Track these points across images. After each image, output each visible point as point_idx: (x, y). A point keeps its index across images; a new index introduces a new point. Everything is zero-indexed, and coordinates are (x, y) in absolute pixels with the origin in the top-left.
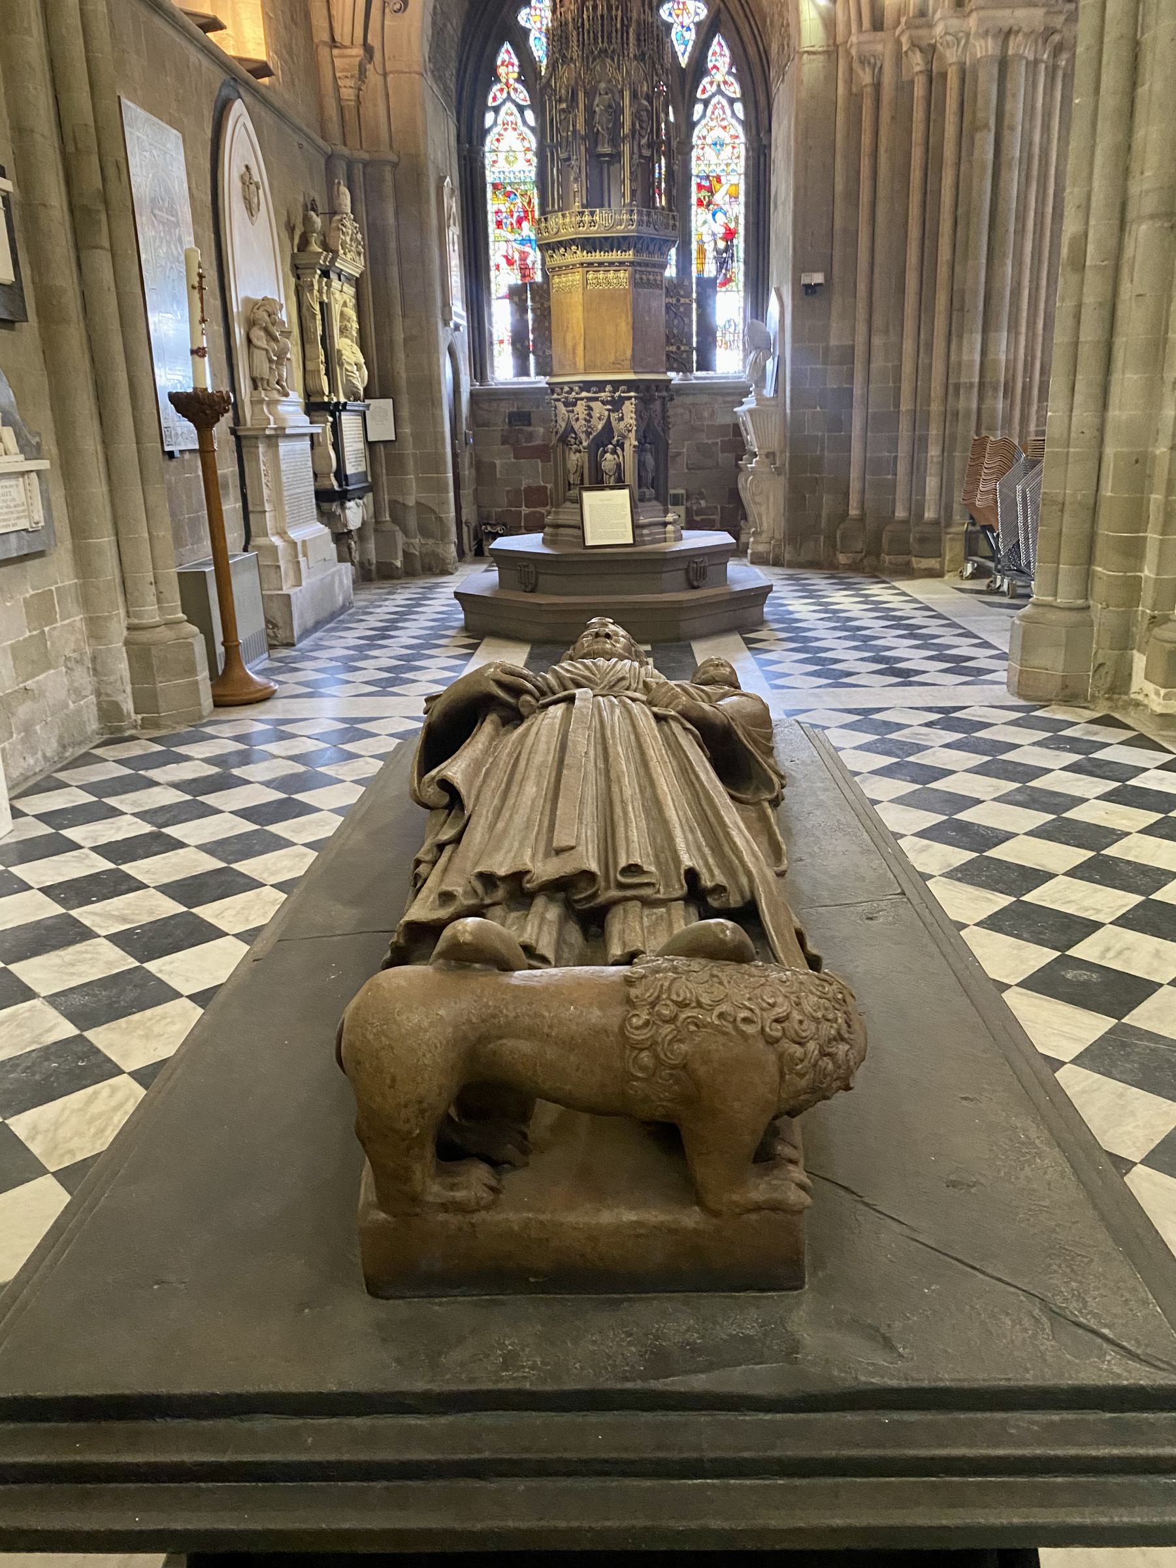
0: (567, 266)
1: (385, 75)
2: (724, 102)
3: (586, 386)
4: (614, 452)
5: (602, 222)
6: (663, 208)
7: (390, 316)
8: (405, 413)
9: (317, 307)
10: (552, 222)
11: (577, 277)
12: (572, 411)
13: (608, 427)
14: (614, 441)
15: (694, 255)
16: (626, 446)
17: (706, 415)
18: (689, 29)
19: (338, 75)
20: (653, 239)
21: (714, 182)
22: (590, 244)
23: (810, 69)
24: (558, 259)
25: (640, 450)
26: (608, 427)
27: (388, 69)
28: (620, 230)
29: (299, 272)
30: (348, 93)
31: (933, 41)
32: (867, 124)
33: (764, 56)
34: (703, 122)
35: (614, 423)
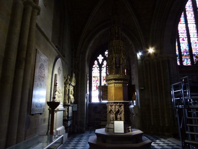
3: (115, 103)
4: (120, 115)
9: (67, 90)
13: (119, 110)
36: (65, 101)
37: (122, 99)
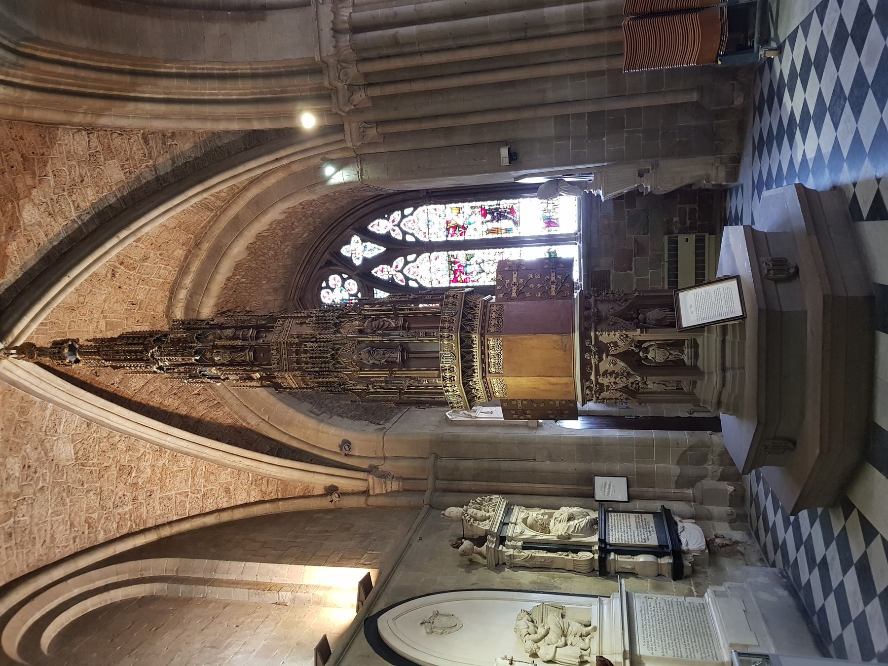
0: (486, 388)
1: (385, 458)
2: (404, 220)
3: (585, 376)
4: (646, 350)
5: (450, 362)
6: (441, 305)
7: (534, 471)
8: (605, 467)
9: (527, 553)
10: (452, 399)
11: (494, 381)
12: (608, 387)
13: (624, 356)
14: (636, 350)
15: (495, 236)
16: (641, 338)
17: (606, 222)
18: (365, 247)
19: (384, 492)
20: (464, 316)
21: (451, 225)
22: (467, 371)
23: (372, 173)
24: (481, 393)
25: (644, 326)
26: (624, 356)
27: (382, 456)
28: (456, 347)
29: (501, 563)
30: (395, 486)
31: (346, 87)
32: (400, 128)
33: (378, 198)
34: (416, 235)
35: (619, 351)
36: (584, 569)
37: (565, 338)
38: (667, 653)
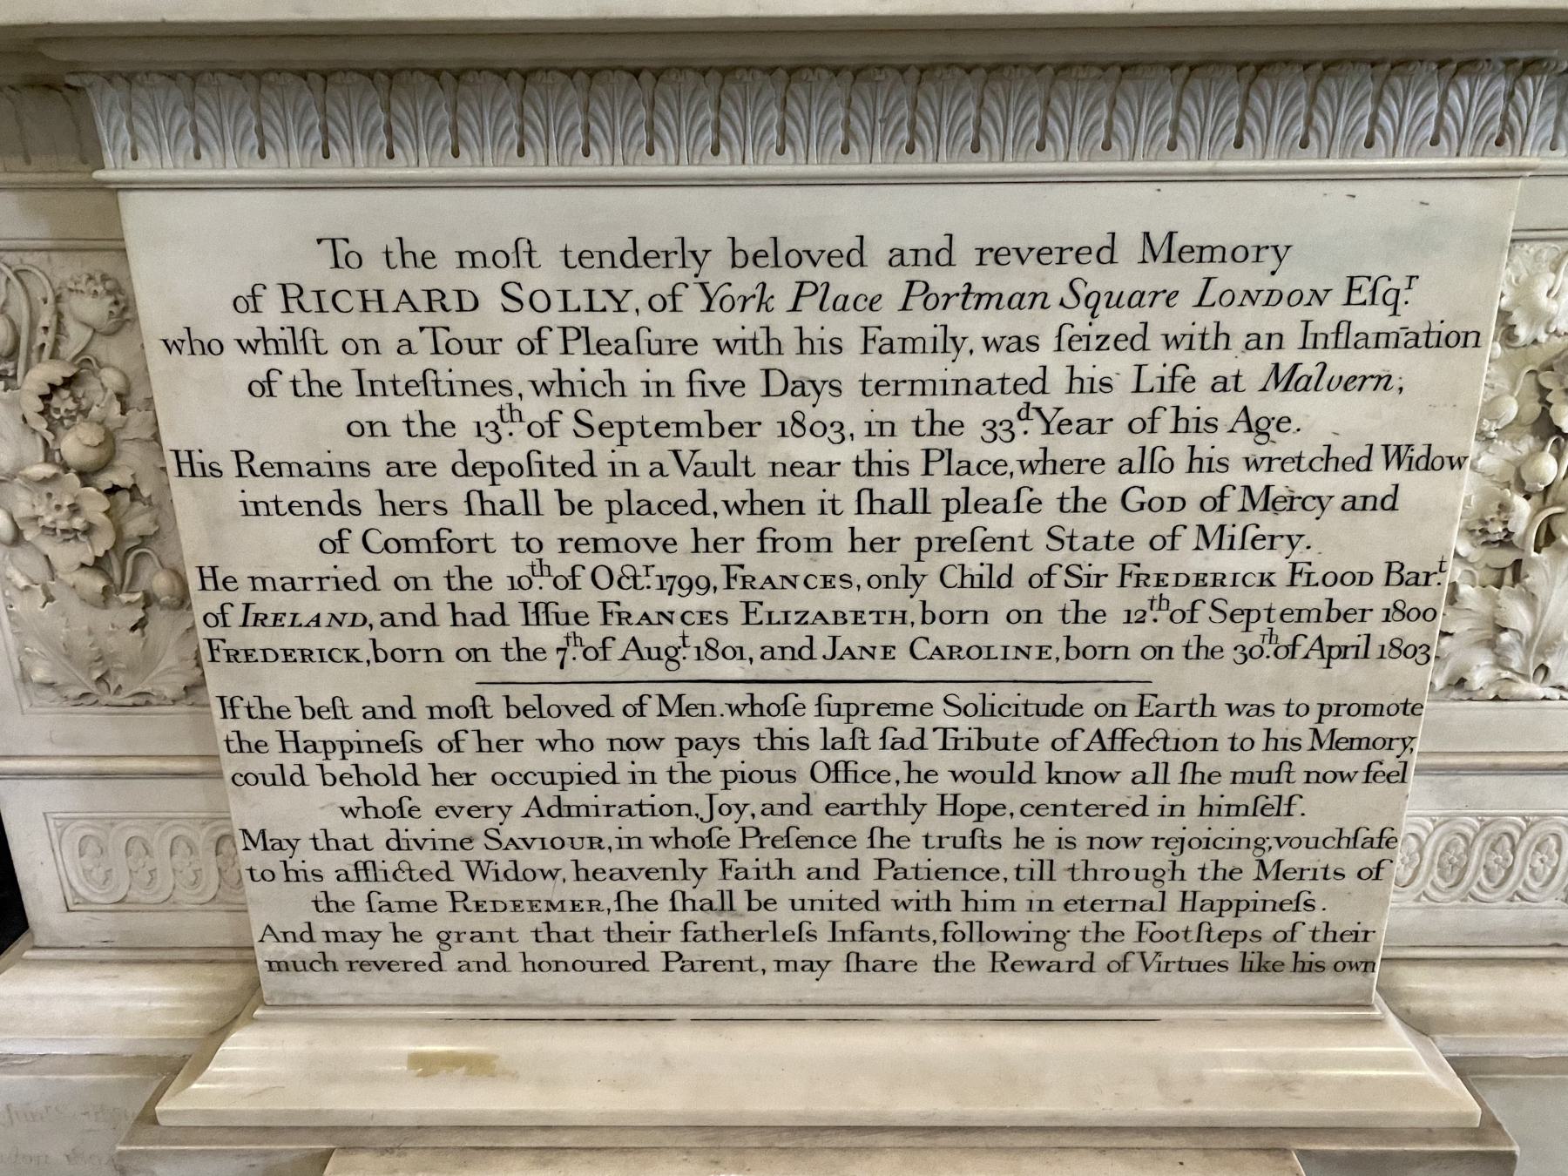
38: (252, 509)
